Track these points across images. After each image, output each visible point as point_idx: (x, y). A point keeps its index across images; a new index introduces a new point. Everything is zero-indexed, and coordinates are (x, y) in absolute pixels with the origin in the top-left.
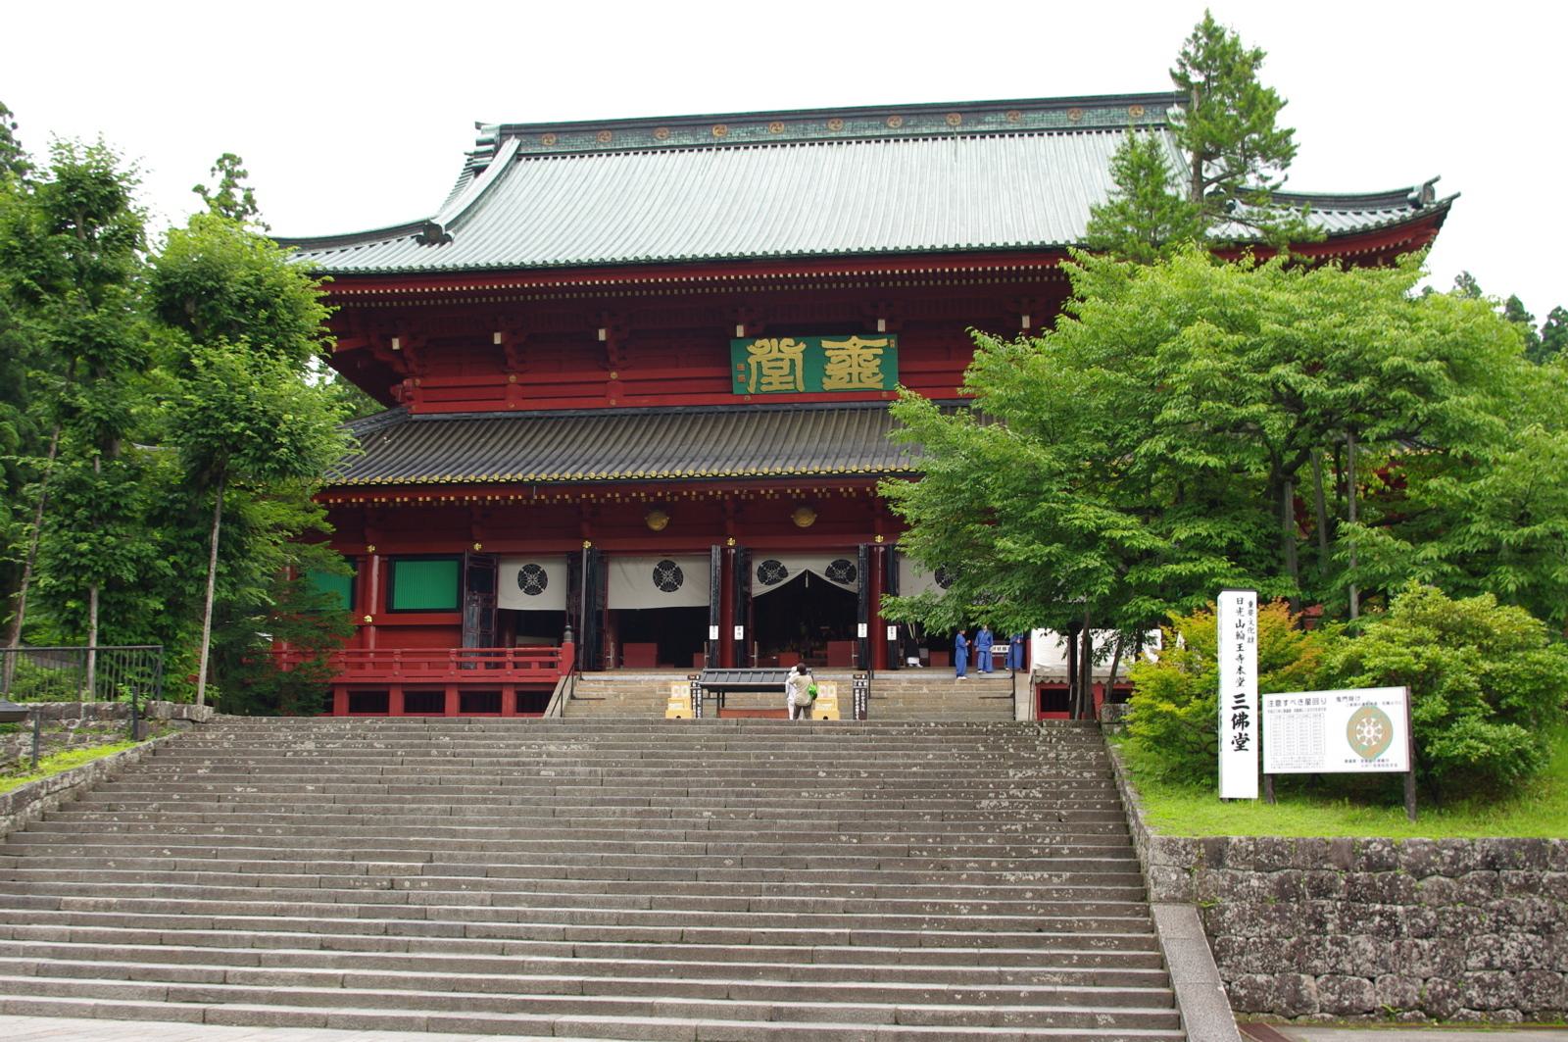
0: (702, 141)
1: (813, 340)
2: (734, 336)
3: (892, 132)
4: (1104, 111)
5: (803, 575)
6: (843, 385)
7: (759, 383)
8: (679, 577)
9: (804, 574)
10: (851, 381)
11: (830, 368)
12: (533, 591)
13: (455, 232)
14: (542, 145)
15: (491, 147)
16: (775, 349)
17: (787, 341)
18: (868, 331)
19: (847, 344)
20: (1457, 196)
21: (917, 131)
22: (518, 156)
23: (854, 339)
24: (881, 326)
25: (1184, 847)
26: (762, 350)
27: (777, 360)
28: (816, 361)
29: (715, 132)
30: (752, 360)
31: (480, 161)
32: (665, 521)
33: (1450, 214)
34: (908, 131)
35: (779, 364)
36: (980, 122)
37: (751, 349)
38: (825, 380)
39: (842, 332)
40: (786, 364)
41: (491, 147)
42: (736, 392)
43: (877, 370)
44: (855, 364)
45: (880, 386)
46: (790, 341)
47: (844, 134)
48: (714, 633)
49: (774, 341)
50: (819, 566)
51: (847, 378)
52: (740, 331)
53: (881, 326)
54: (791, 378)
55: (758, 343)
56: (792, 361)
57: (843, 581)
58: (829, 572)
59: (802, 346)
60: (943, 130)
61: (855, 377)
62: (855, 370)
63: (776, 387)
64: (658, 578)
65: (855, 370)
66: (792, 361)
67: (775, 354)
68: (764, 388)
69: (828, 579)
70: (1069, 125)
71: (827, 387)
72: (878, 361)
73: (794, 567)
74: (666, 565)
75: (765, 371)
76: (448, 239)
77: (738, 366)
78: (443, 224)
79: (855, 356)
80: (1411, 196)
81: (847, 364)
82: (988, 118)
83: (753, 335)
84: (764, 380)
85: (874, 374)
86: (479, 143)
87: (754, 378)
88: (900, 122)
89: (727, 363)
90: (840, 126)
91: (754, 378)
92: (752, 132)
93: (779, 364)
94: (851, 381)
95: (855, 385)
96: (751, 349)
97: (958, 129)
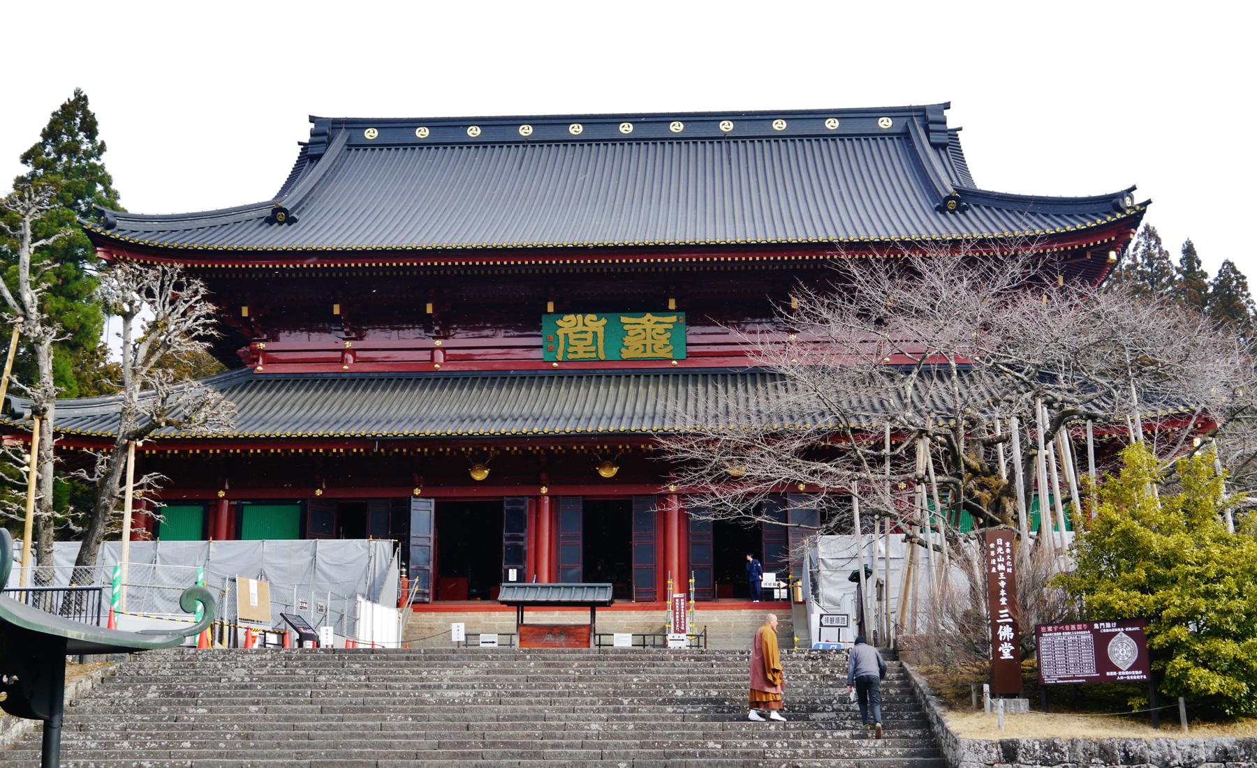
1: (613, 316)
6: (638, 355)
7: (566, 352)
10: (645, 351)
13: (298, 214)
15: (325, 138)
16: (580, 323)
17: (590, 317)
18: (662, 309)
19: (643, 320)
23: (649, 315)
24: (672, 305)
25: (986, 747)
26: (570, 324)
27: (581, 332)
28: (616, 335)
30: (560, 332)
31: (313, 151)
37: (559, 323)
38: (623, 350)
40: (590, 336)
41: (325, 138)
44: (649, 337)
46: (594, 317)
49: (580, 316)
51: (642, 349)
52: (550, 307)
53: (672, 305)
54: (593, 348)
55: (566, 318)
56: (595, 333)
59: (604, 321)
61: (649, 348)
62: (649, 342)
63: (580, 355)
65: (649, 342)
66: (595, 333)
67: (580, 327)
68: (570, 356)
71: (624, 357)
72: (668, 335)
75: (572, 342)
76: (294, 220)
78: (289, 208)
79: (649, 330)
83: (561, 310)
84: (571, 349)
95: (649, 354)
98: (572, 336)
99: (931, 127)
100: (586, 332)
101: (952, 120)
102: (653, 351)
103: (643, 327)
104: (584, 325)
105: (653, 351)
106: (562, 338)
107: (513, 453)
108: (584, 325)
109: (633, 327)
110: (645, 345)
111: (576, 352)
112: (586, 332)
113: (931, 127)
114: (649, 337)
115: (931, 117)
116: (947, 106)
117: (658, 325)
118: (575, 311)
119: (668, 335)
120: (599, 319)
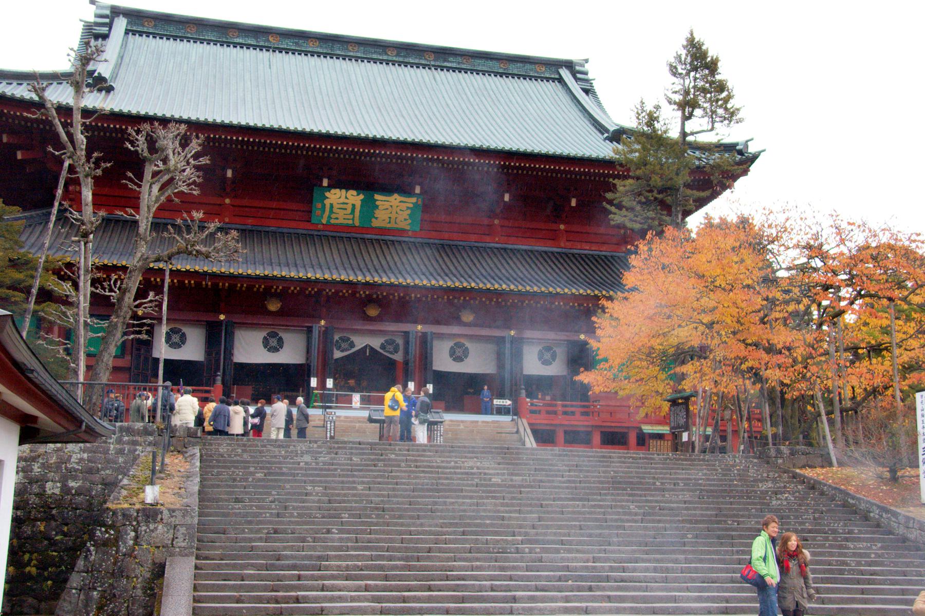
0: (262, 43)
2: (321, 185)
3: (390, 58)
4: (521, 65)
7: (330, 217)
8: (281, 342)
9: (366, 346)
10: (390, 222)
11: (378, 213)
14: (144, 26)
15: (107, 20)
20: (764, 151)
21: (407, 60)
22: (127, 32)
23: (396, 196)
27: (344, 203)
28: (369, 207)
29: (271, 39)
30: (327, 202)
32: (279, 305)
33: (757, 161)
34: (401, 59)
35: (345, 206)
36: (445, 61)
37: (327, 194)
38: (374, 220)
39: (388, 190)
40: (349, 207)
41: (107, 20)
42: (313, 221)
43: (407, 217)
44: (394, 212)
45: (408, 228)
46: (354, 192)
47: (359, 55)
48: (314, 382)
49: (344, 191)
50: (376, 343)
51: (388, 220)
52: (325, 183)
53: (418, 190)
55: (333, 191)
56: (354, 206)
57: (391, 353)
58: (383, 347)
59: (362, 197)
60: (423, 62)
61: (393, 220)
63: (341, 221)
64: (266, 343)
65: (393, 216)
66: (354, 206)
67: (343, 200)
68: (333, 221)
69: (381, 351)
70: (501, 71)
72: (409, 212)
73: (360, 342)
74: (273, 335)
75: (335, 210)
77: (317, 205)
80: (738, 148)
81: (389, 211)
82: (451, 59)
83: (331, 186)
84: (333, 216)
85: (405, 220)
88: (395, 53)
89: (310, 202)
90: (356, 49)
93: (345, 206)
94: (390, 222)
96: (327, 194)
97: (433, 63)
98: (336, 206)
101: (593, 71)
102: (396, 223)
104: (346, 198)
106: (328, 206)
108: (346, 198)
109: (384, 203)
111: (337, 218)
112: (347, 204)
113: (579, 76)
114: (394, 212)
115: (578, 68)
116: (587, 61)
118: (341, 188)
120: (358, 195)
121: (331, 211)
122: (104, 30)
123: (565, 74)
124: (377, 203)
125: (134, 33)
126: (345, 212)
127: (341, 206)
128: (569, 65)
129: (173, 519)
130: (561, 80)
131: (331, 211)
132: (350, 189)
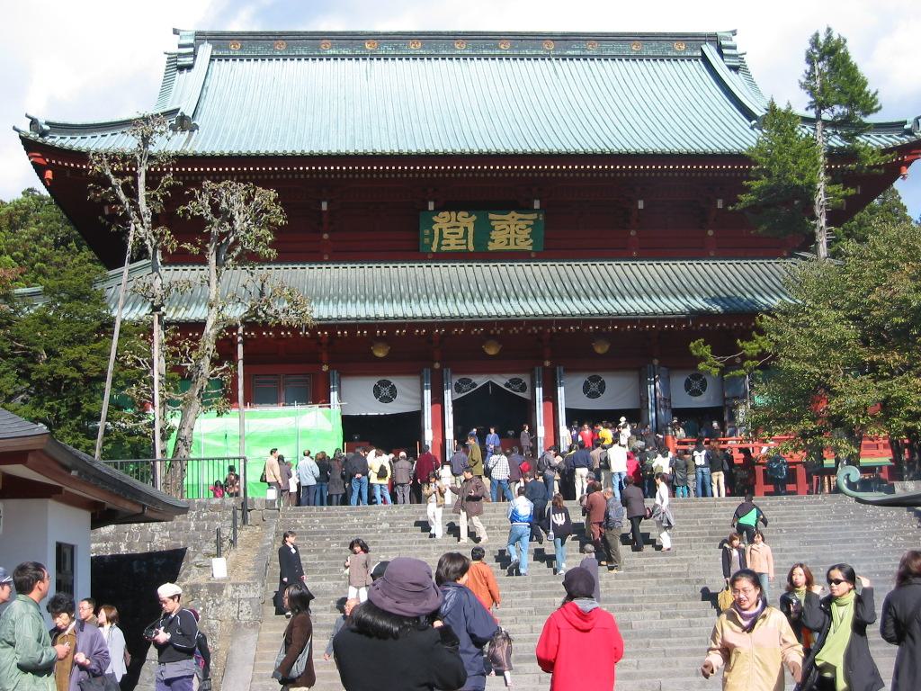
0: (357, 52)
5: (486, 386)
7: (440, 245)
10: (508, 244)
12: (593, 395)
14: (229, 50)
15: (191, 50)
16: (453, 219)
17: (461, 214)
18: (525, 208)
22: (212, 59)
24: (537, 205)
30: (436, 228)
37: (435, 219)
38: (490, 243)
39: (504, 207)
40: (461, 231)
41: (191, 50)
43: (528, 237)
45: (530, 248)
46: (466, 214)
49: (453, 214)
50: (501, 381)
52: (431, 206)
53: (537, 205)
54: (464, 241)
55: (441, 214)
56: (466, 228)
61: (512, 241)
62: (512, 236)
63: (453, 247)
65: (512, 236)
66: (466, 228)
67: (453, 223)
68: (443, 248)
71: (490, 248)
72: (530, 230)
73: (480, 381)
75: (445, 235)
83: (438, 210)
84: (443, 242)
85: (527, 240)
86: (181, 46)
87: (436, 239)
89: (417, 229)
91: (436, 239)
92: (396, 47)
94: (508, 244)
95: (512, 247)
96: (435, 219)
98: (445, 232)
99: (725, 51)
100: (458, 227)
101: (742, 44)
102: (516, 244)
103: (508, 223)
104: (457, 221)
105: (516, 244)
106: (437, 232)
107: (403, 334)
108: (457, 221)
110: (509, 239)
111: (449, 245)
112: (458, 227)
113: (725, 51)
116: (734, 33)
117: (521, 222)
118: (450, 210)
119: (530, 230)
120: (469, 217)
121: (441, 238)
122: (189, 60)
123: (710, 51)
124: (493, 223)
125: (220, 58)
126: (457, 236)
127: (452, 230)
128: (714, 39)
129: (237, 594)
130: (705, 59)
131: (441, 238)
132: (461, 210)
